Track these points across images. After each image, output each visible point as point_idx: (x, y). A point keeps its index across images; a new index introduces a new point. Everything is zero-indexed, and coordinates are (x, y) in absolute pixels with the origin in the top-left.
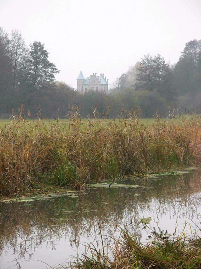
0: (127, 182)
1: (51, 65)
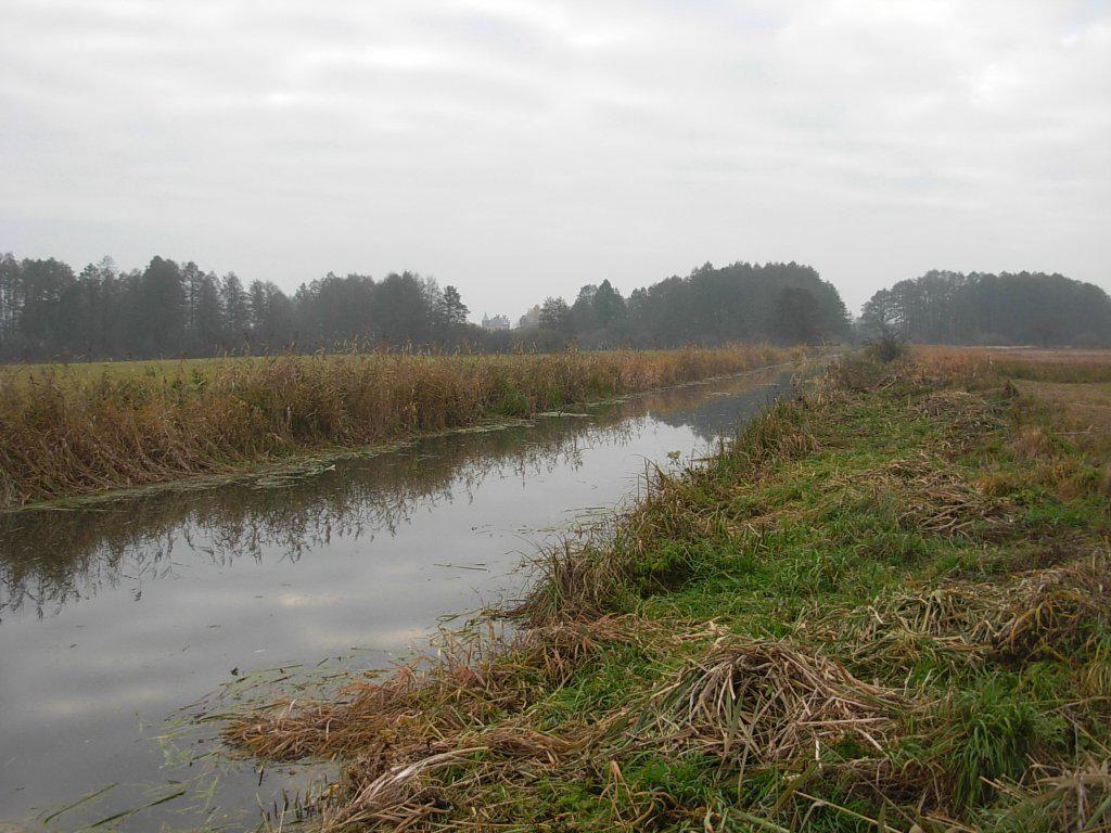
0: (569, 411)
1: (463, 307)
